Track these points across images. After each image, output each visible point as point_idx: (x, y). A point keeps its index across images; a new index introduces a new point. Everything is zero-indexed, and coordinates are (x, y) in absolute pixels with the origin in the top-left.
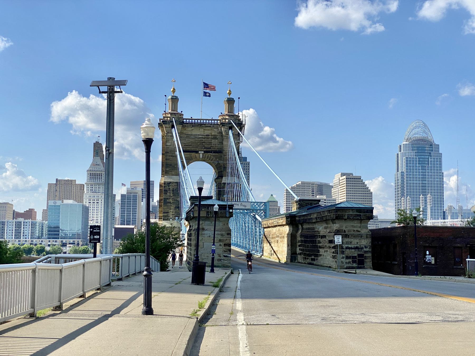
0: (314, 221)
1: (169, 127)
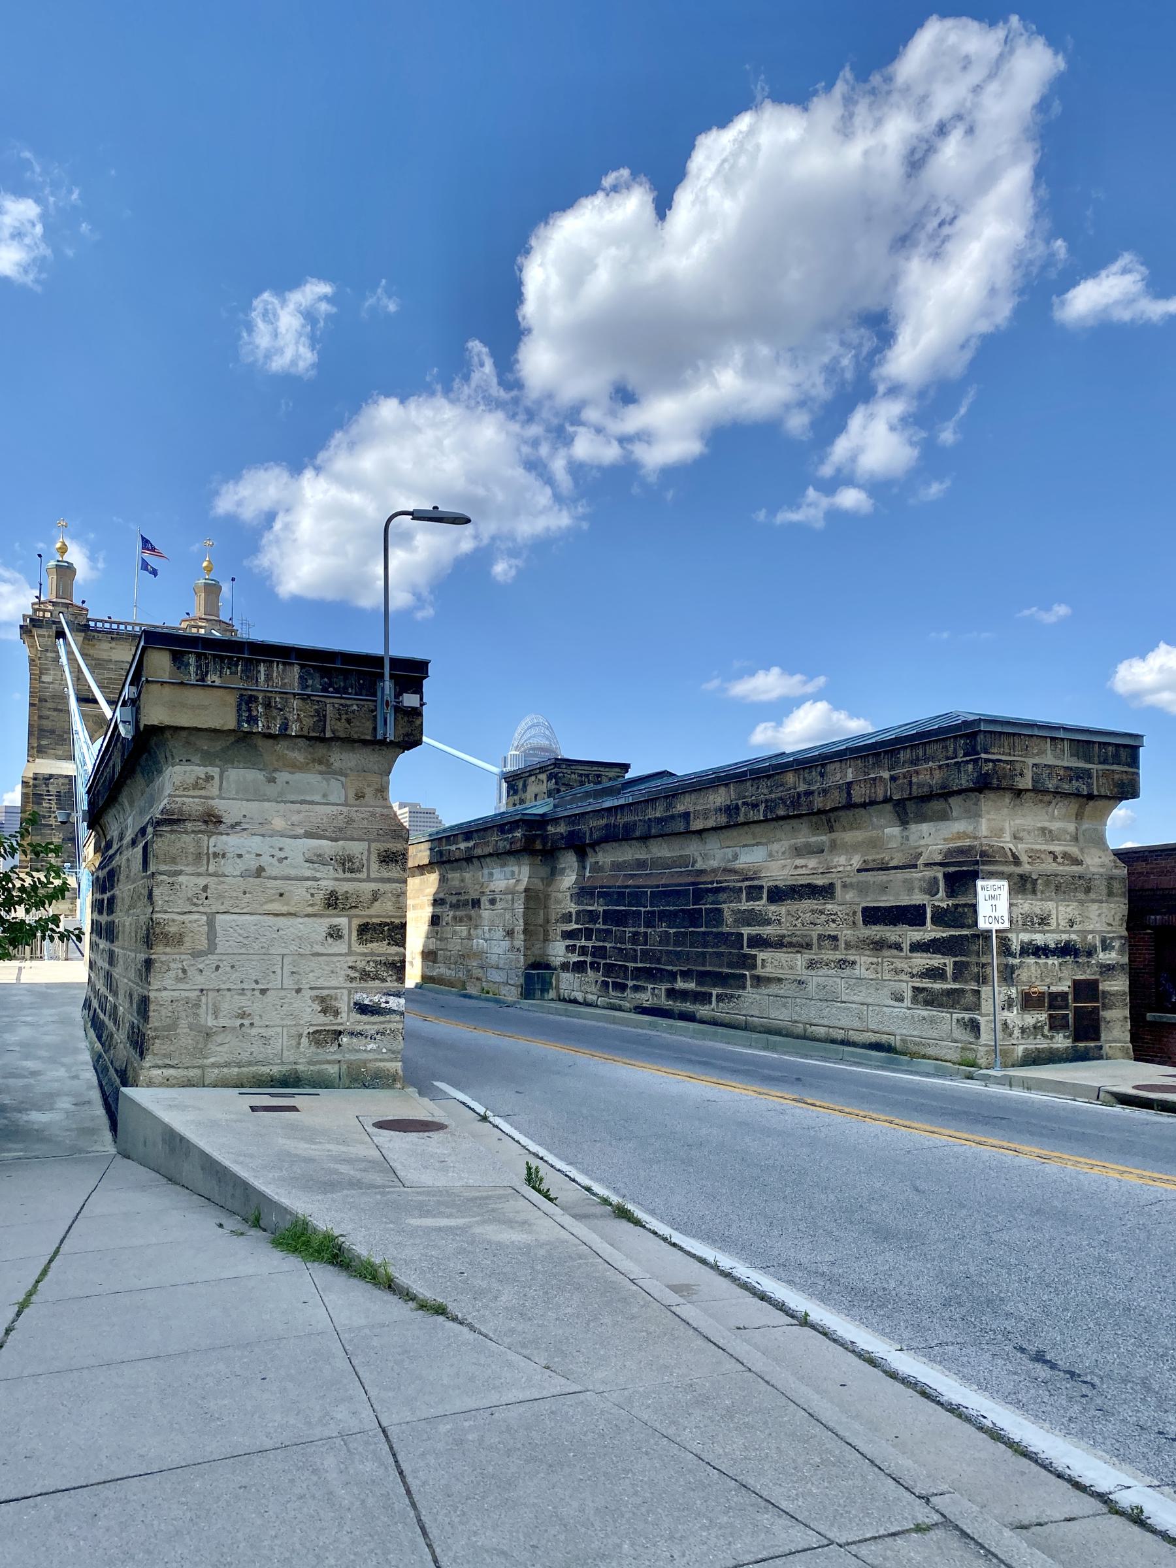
0: (697, 825)
1: (49, 636)
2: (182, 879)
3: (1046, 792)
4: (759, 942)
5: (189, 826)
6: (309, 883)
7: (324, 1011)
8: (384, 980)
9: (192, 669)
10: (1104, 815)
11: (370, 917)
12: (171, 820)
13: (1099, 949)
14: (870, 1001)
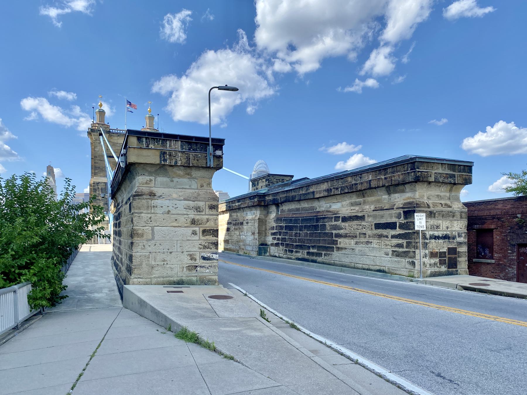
0: (317, 196)
2: (142, 215)
3: (439, 182)
4: (339, 236)
5: (145, 197)
6: (185, 216)
7: (191, 259)
8: (211, 249)
9: (144, 143)
10: (459, 191)
11: (206, 227)
12: (138, 195)
13: (457, 237)
14: (377, 255)
